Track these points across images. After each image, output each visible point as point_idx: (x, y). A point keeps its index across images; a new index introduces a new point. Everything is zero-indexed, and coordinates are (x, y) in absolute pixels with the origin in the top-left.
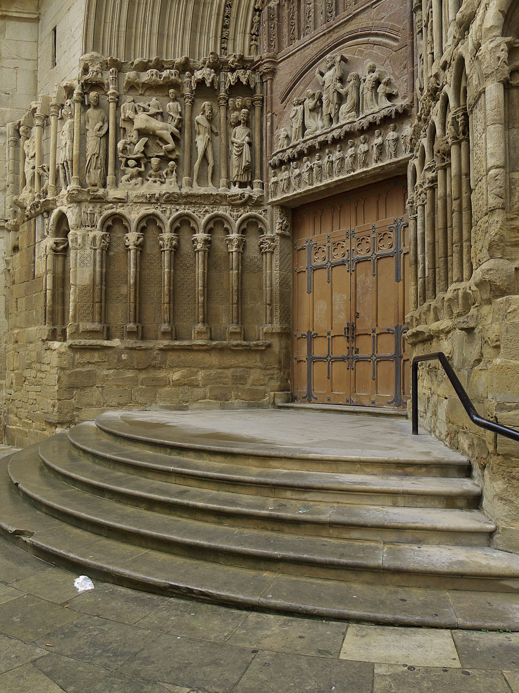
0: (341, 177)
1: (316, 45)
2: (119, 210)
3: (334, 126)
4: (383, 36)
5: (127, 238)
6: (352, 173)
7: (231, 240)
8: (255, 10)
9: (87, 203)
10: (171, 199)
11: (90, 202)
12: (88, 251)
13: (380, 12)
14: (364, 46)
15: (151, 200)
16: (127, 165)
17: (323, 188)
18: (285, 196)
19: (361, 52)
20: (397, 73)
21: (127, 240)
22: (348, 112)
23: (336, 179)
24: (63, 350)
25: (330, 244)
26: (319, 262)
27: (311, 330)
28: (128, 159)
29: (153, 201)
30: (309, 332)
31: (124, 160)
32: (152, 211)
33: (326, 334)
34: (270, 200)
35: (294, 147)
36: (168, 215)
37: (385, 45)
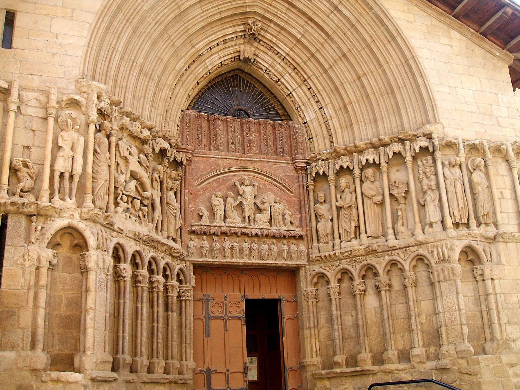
0: (258, 261)
1: (228, 162)
2: (122, 241)
3: (253, 226)
4: (284, 186)
5: (124, 269)
6: (267, 262)
7: (173, 286)
8: (182, 111)
9: (99, 226)
10: (150, 242)
11: (102, 225)
12: (104, 276)
13: (278, 169)
14: (267, 183)
15: (137, 238)
16: (121, 199)
17: (241, 264)
18: (206, 259)
19: (265, 186)
20: (291, 210)
21: (124, 271)
22: (266, 222)
23: (253, 261)
24: (84, 382)
25: (225, 302)
26: (217, 314)
27: (210, 367)
28: (123, 194)
29: (137, 239)
30: (209, 369)
31: (121, 194)
32: (138, 248)
33: (225, 371)
34: (189, 258)
35: (219, 227)
36: (148, 254)
37: (284, 191)
